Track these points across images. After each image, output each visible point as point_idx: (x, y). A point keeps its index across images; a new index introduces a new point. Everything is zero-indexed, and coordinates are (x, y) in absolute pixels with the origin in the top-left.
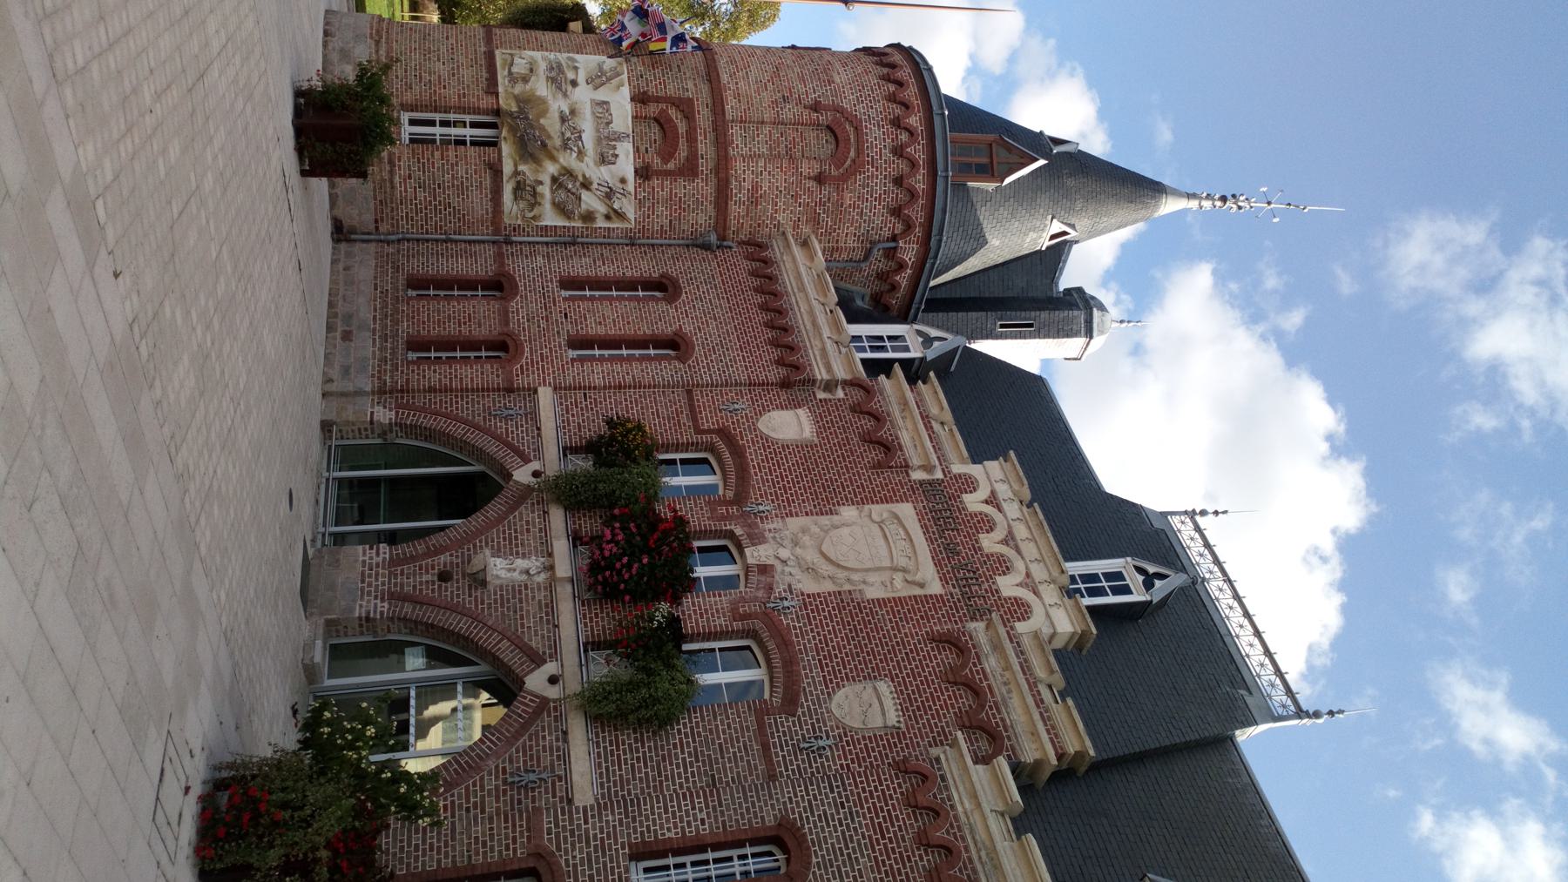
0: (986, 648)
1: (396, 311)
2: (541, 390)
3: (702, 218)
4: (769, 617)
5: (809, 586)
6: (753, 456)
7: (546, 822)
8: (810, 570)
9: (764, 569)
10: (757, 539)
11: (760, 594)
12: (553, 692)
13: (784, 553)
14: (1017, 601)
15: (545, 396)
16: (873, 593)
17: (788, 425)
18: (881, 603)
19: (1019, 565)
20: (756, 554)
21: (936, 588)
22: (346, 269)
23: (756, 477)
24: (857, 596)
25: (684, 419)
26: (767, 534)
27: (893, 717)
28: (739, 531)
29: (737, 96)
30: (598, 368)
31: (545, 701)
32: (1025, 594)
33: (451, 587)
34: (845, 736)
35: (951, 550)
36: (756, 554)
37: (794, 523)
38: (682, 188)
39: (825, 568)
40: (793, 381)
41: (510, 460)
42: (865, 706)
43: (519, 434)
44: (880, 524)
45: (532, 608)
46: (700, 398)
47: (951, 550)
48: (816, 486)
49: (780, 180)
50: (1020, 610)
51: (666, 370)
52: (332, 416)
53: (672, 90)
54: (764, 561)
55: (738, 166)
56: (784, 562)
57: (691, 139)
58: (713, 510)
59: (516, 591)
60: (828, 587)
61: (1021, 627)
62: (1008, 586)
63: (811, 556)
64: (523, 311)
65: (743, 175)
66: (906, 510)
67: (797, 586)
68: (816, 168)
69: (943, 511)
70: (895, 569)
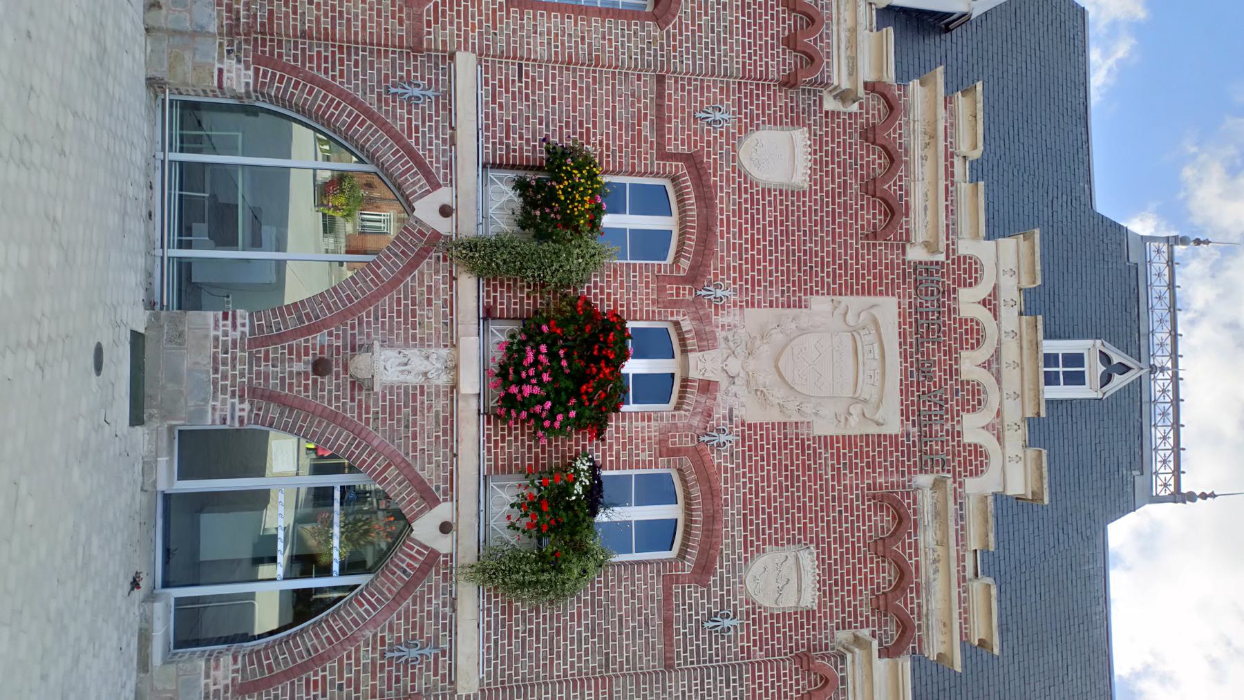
2: (460, 56)
5: (752, 413)
6: (726, 202)
8: (761, 394)
9: (707, 387)
10: (706, 341)
11: (696, 421)
12: (443, 545)
13: (734, 366)
14: (978, 451)
15: (466, 63)
16: (824, 428)
18: (828, 442)
19: (993, 399)
20: (702, 365)
24: (803, 431)
25: (647, 130)
26: (720, 334)
27: (809, 599)
28: (686, 325)
31: (434, 554)
32: (987, 441)
33: (329, 382)
34: (754, 614)
36: (702, 365)
39: (778, 394)
42: (780, 579)
43: (429, 146)
44: (854, 332)
45: (426, 422)
47: (923, 371)
50: (975, 460)
52: (161, 72)
54: (710, 376)
58: (661, 290)
59: (412, 395)
60: (777, 417)
62: (973, 428)
63: (766, 377)
66: (887, 309)
69: (933, 335)
70: (855, 400)
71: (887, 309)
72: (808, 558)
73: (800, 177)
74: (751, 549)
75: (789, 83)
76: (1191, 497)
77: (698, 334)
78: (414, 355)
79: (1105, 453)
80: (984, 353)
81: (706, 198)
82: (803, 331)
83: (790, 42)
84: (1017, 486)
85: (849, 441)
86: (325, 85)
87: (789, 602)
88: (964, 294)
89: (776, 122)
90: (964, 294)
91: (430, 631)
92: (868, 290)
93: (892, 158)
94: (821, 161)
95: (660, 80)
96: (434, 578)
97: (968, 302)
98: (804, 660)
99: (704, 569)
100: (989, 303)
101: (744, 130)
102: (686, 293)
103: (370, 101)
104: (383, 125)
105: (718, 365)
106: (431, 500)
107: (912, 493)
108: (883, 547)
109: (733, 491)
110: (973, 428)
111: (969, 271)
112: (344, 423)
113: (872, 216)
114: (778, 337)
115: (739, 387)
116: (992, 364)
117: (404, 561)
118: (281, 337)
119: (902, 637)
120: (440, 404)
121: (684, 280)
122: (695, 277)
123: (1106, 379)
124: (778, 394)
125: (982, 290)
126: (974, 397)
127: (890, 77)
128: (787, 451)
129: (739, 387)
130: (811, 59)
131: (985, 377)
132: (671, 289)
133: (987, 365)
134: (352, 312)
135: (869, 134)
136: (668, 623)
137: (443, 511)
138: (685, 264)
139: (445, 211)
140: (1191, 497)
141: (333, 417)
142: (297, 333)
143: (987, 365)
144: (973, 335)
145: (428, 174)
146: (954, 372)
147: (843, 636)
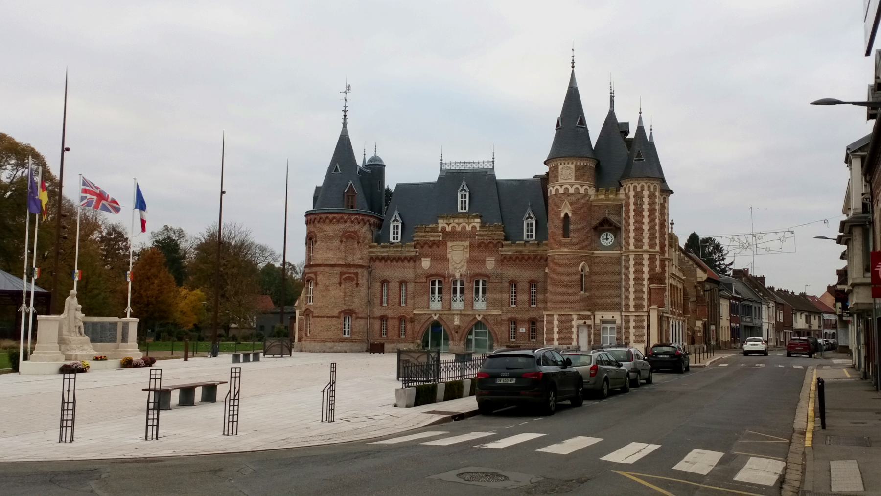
3: (365, 272)
4: (471, 277)
8: (463, 266)
9: (461, 275)
10: (454, 276)
15: (415, 312)
16: (468, 256)
17: (426, 263)
20: (457, 276)
21: (467, 243)
23: (439, 272)
27: (493, 259)
30: (408, 300)
32: (471, 225)
35: (460, 237)
36: (457, 276)
38: (360, 277)
40: (415, 260)
41: (431, 320)
43: (426, 318)
47: (460, 237)
48: (441, 259)
50: (474, 228)
51: (410, 287)
53: (338, 276)
55: (355, 262)
61: (478, 229)
62: (469, 228)
63: (460, 265)
64: (390, 314)
66: (450, 244)
71: (450, 244)
72: (487, 259)
73: (429, 259)
75: (415, 261)
83: (409, 261)
93: (426, 243)
94: (427, 256)
98: (502, 261)
99: (488, 276)
100: (448, 224)
108: (487, 246)
109: (477, 271)
111: (444, 228)
113: (435, 246)
116: (458, 224)
117: (483, 321)
122: (444, 277)
125: (446, 226)
126: (464, 228)
130: (411, 258)
135: (422, 247)
144: (454, 228)
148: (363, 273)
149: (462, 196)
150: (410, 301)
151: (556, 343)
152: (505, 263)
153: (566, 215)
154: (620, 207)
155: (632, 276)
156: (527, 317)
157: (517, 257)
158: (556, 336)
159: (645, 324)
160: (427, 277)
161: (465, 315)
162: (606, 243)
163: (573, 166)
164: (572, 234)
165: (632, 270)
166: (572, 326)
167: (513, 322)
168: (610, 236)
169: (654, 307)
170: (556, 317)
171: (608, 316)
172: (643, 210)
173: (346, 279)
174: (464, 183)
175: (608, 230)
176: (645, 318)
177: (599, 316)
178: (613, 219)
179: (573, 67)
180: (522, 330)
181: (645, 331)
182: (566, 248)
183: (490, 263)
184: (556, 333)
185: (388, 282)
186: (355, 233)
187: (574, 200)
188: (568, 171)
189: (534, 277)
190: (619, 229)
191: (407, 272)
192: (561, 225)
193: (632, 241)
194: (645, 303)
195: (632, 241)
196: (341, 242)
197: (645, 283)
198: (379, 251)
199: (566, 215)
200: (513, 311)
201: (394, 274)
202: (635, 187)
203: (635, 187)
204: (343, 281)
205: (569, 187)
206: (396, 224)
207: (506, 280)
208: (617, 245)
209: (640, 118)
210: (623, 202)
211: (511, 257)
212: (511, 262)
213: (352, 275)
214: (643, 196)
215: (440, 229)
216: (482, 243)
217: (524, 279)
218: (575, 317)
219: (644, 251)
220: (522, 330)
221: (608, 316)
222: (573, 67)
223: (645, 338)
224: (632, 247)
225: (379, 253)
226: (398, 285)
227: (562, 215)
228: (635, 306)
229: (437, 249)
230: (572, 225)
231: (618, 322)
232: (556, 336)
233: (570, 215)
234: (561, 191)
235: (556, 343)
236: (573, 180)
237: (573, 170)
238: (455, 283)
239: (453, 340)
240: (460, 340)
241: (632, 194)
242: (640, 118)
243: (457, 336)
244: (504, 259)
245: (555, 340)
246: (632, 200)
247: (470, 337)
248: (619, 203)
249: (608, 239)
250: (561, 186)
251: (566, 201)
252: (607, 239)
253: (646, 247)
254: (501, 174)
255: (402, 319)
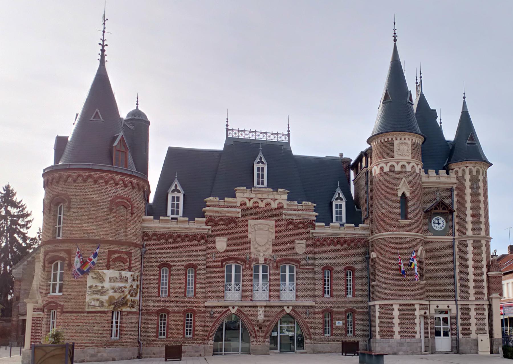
0: (291, 217)
1: (172, 341)
5: (270, 251)
7: (317, 310)
8: (267, 249)
10: (257, 260)
11: (272, 262)
13: (262, 254)
14: (279, 204)
15: (206, 304)
17: (221, 244)
18: (276, 236)
19: (269, 200)
20: (261, 260)
21: (273, 223)
22: (154, 354)
23: (237, 256)
24: (274, 241)
25: (218, 270)
26: (256, 257)
27: (304, 242)
29: (106, 235)
31: (292, 309)
32: (277, 202)
33: (263, 327)
36: (261, 260)
37: (252, 250)
39: (267, 246)
40: (206, 239)
44: (255, 230)
45: (270, 311)
46: (210, 264)
47: (263, 215)
49: (132, 226)
51: (200, 273)
56: (264, 255)
57: (122, 252)
58: (247, 268)
59: (266, 314)
60: (271, 247)
62: (274, 205)
63: (264, 248)
64: (172, 307)
65: (131, 238)
67: (270, 253)
68: (129, 214)
71: (251, 222)
72: (297, 241)
73: (225, 239)
74: (295, 252)
75: (206, 241)
76: (289, 131)
77: (256, 261)
78: (259, 313)
79: (277, 153)
80: (260, 202)
81: (230, 259)
82: (255, 240)
84: (286, 197)
85: (276, 232)
86: (212, 328)
87: (304, 246)
88: (248, 205)
89: (214, 244)
90: (248, 205)
91: (305, 310)
92: (247, 226)
93: (222, 220)
94: (222, 236)
95: (207, 267)
96: (296, 309)
97: (250, 204)
98: (315, 244)
99: (298, 262)
100: (250, 199)
101: (216, 250)
102: (248, 263)
103: (214, 321)
104: (218, 318)
105: (261, 257)
106: (284, 310)
107: (286, 220)
108: (296, 227)
109: (284, 255)
110: (274, 205)
111: (243, 203)
112: (270, 324)
113: (232, 224)
114: (256, 246)
115: (266, 254)
116: (262, 200)
118: (256, 334)
119: (311, 224)
120: (267, 309)
121: (246, 264)
122: (245, 261)
123: (263, 163)
124: (267, 246)
125: (247, 201)
126: (268, 204)
127: (204, 219)
128: (278, 243)
129: (266, 254)
130: (203, 237)
131: (265, 201)
132: (247, 266)
133: (262, 201)
134: (251, 324)
135: (216, 224)
136: (307, 269)
137: (285, 308)
138: (242, 263)
139: (233, 308)
140: (289, 131)
141: (269, 326)
142: (255, 332)
143: (262, 201)
144: (256, 203)
145: (227, 311)
146: (263, 209)
147: (311, 236)
148: (136, 252)
149: (261, 167)
150: (201, 291)
151: (397, 336)
152: (318, 247)
153: (403, 194)
154: (451, 190)
155: (471, 263)
156: (343, 309)
157: (332, 241)
158: (397, 329)
159: (486, 313)
160: (222, 261)
161: (271, 307)
162: (437, 227)
163: (409, 142)
164: (410, 215)
165: (470, 256)
166: (414, 317)
167: (329, 313)
168: (441, 220)
169: (494, 295)
170: (396, 307)
171: (443, 305)
172: (479, 194)
173: (114, 260)
174: (261, 155)
175: (442, 215)
176: (486, 307)
177: (433, 305)
178: (446, 200)
179: (395, 40)
180: (339, 323)
181: (486, 321)
182: (405, 230)
183: (300, 247)
184: (396, 325)
185: (169, 266)
186: (129, 201)
187: (411, 179)
188: (406, 147)
189: (350, 264)
190: (452, 212)
191: (197, 254)
192: (398, 205)
193: (469, 226)
194: (485, 291)
195: (469, 226)
196: (111, 210)
197: (484, 270)
198: (154, 225)
199: (403, 194)
200: (326, 301)
201: (179, 258)
202: (471, 171)
203: (471, 171)
204: (111, 263)
205: (406, 164)
206: (176, 194)
207: (318, 267)
208: (449, 230)
209: (464, 103)
210: (455, 186)
211: (325, 240)
212: (326, 246)
213: (125, 256)
214: (479, 181)
215: (239, 205)
216: (291, 222)
217: (339, 265)
218: (417, 307)
219: (481, 237)
220: (339, 323)
221: (443, 305)
222: (395, 40)
223: (487, 328)
224: (470, 233)
225: (157, 230)
226: (183, 271)
227: (400, 194)
228: (475, 295)
229: (234, 227)
230: (411, 205)
231: (454, 312)
232: (397, 329)
233: (408, 194)
234: (398, 168)
235: (397, 336)
236: (410, 158)
237: (410, 146)
238: (257, 269)
239: (256, 338)
240: (265, 338)
241: (467, 177)
242: (464, 103)
243: (261, 334)
244: (318, 242)
245: (396, 333)
246: (468, 184)
247: (274, 334)
248: (449, 186)
249: (439, 224)
250: (398, 163)
251: (404, 179)
252: (439, 224)
253: (470, 233)
254: (297, 150)
255: (190, 313)
